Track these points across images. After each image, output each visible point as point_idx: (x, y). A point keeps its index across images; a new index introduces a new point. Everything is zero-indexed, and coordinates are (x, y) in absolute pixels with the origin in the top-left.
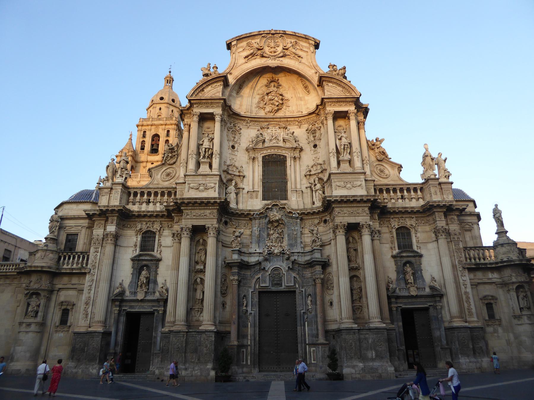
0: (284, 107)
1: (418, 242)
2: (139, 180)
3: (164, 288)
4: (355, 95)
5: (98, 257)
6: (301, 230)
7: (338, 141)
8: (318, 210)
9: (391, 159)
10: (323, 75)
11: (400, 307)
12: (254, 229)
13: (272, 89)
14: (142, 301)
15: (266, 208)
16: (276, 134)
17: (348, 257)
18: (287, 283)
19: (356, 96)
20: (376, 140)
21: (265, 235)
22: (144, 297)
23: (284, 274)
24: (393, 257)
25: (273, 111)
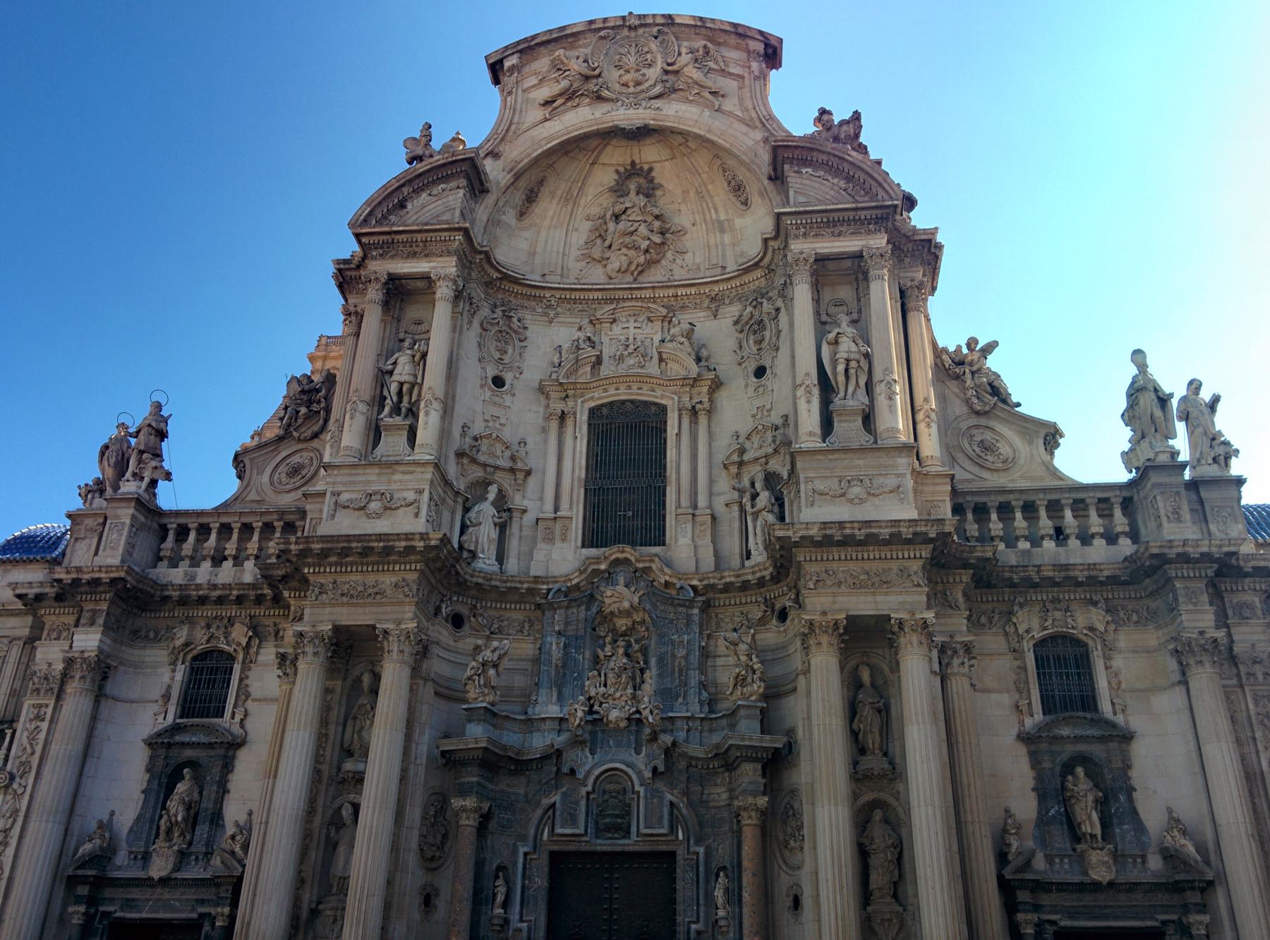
0: (669, 255)
1: (1115, 688)
3: (238, 838)
4: (886, 197)
5: (42, 736)
6: (703, 644)
7: (826, 350)
8: (758, 575)
9: (1018, 405)
10: (783, 141)
11: (1053, 923)
12: (549, 639)
13: (634, 199)
14: (164, 881)
15: (590, 570)
16: (639, 337)
17: (854, 735)
19: (890, 203)
20: (968, 345)
21: (584, 657)
22: (177, 868)
23: (639, 792)
24: (1025, 738)
25: (633, 268)
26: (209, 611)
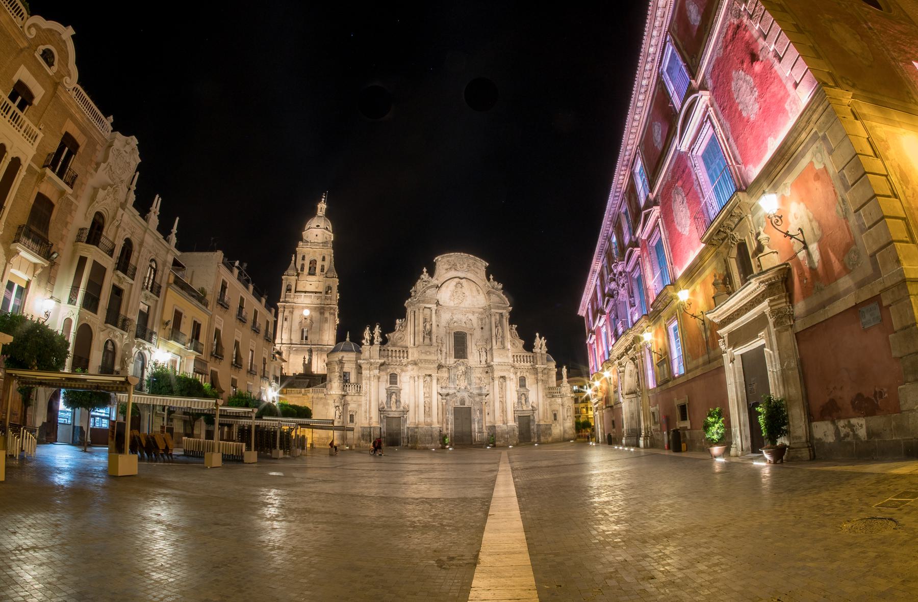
13: (459, 289)
18: (467, 404)
24: (517, 391)
26: (392, 366)
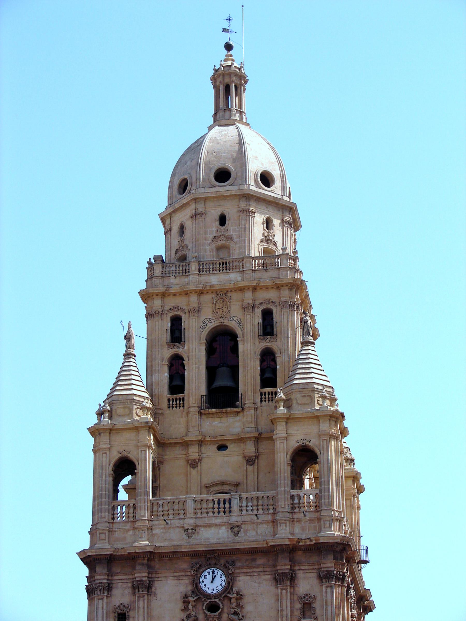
2: (192, 521)
